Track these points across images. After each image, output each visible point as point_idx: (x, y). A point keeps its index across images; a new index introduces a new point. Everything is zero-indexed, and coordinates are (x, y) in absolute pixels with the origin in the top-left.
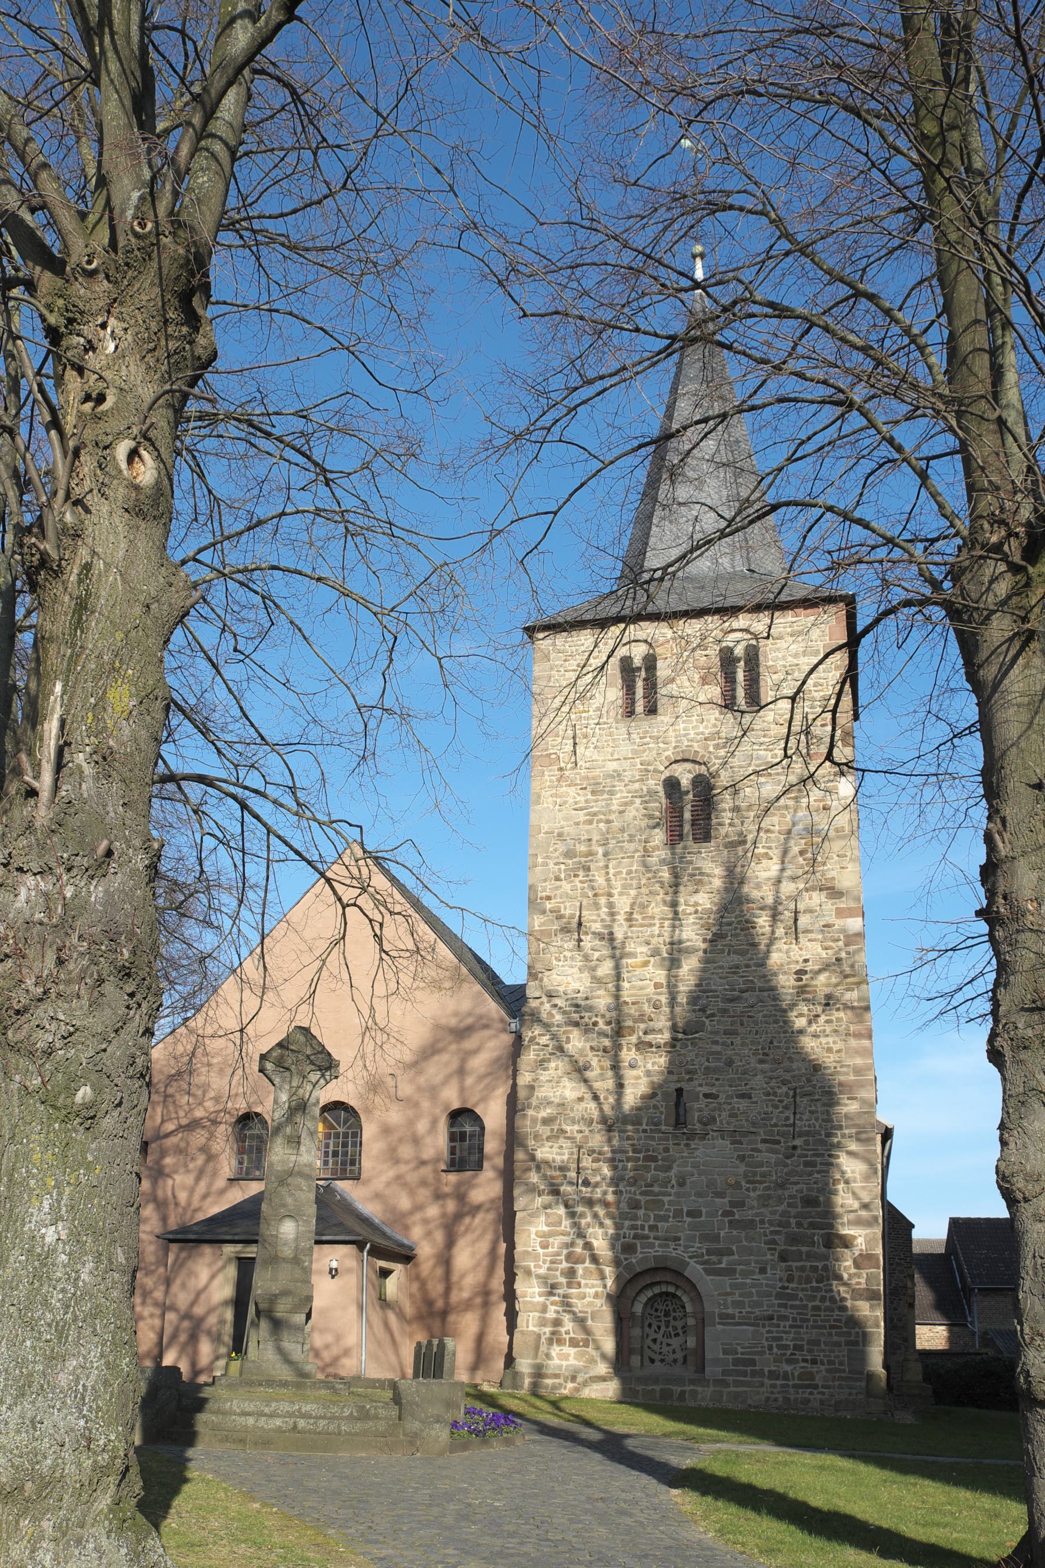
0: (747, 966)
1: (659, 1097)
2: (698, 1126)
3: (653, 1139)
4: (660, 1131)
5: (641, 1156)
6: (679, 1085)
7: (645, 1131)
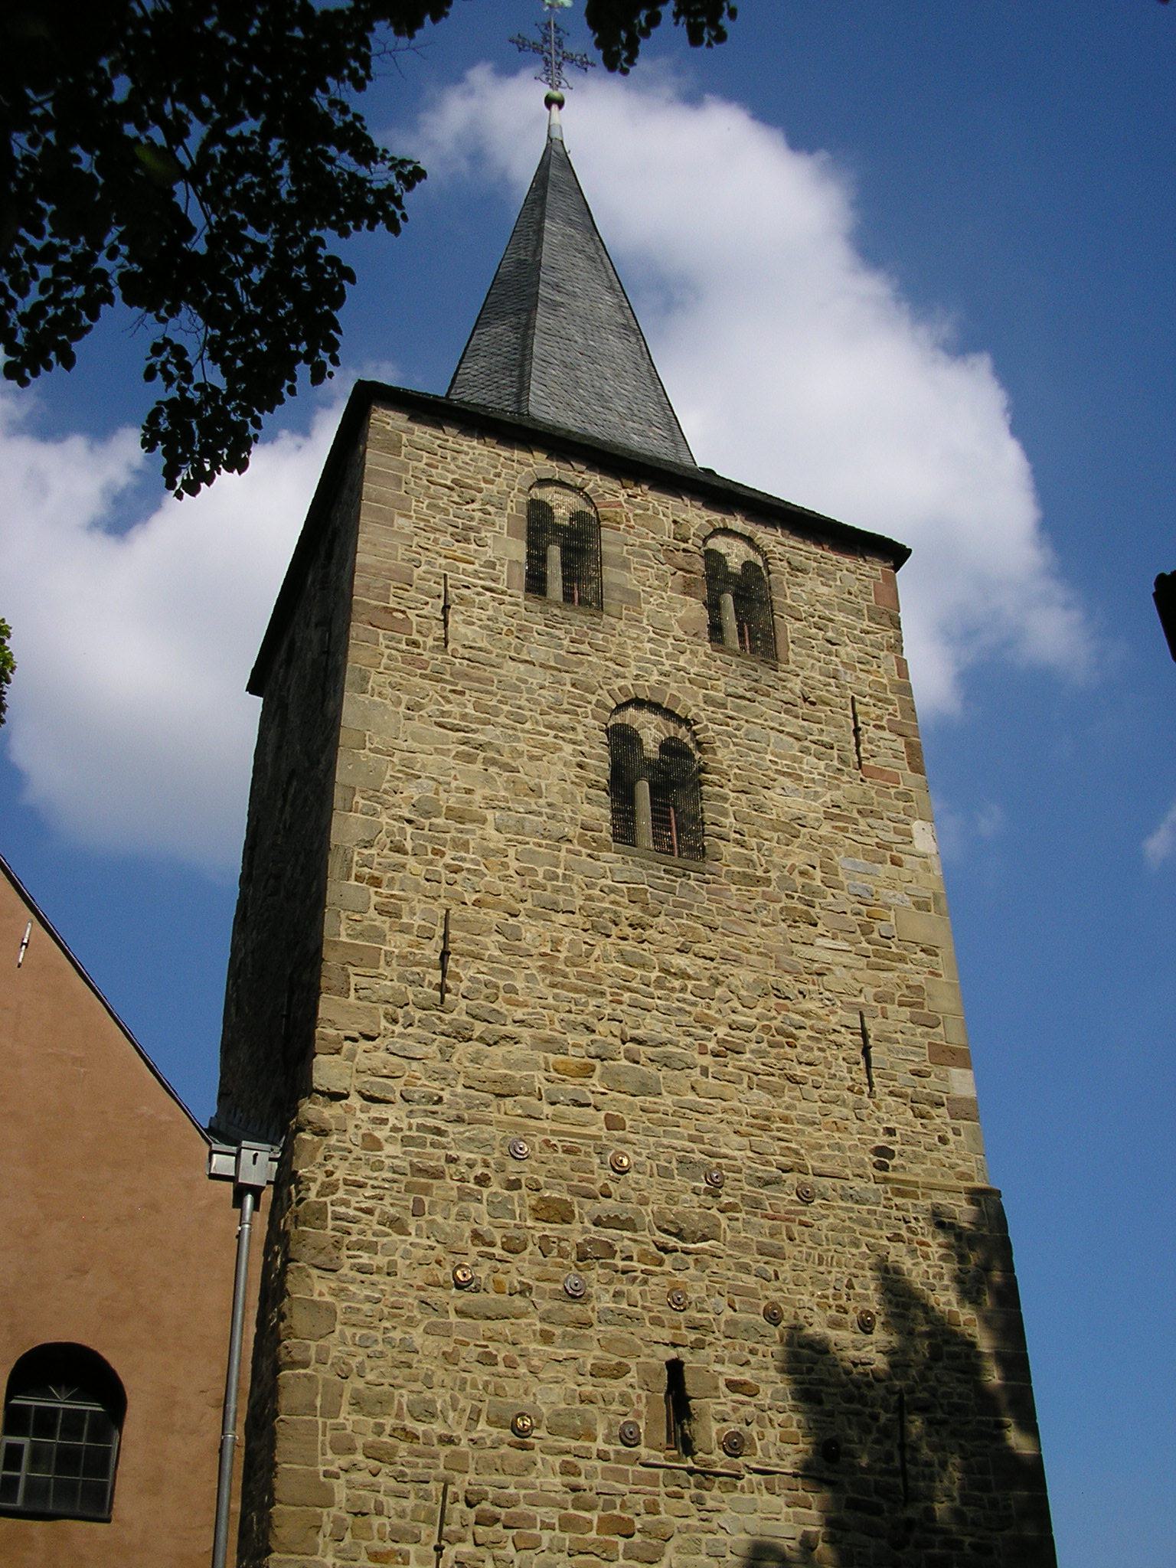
0: (785, 1120)
1: (632, 1377)
2: (718, 1455)
3: (621, 1476)
4: (636, 1459)
5: (594, 1516)
6: (672, 1354)
7: (603, 1456)
